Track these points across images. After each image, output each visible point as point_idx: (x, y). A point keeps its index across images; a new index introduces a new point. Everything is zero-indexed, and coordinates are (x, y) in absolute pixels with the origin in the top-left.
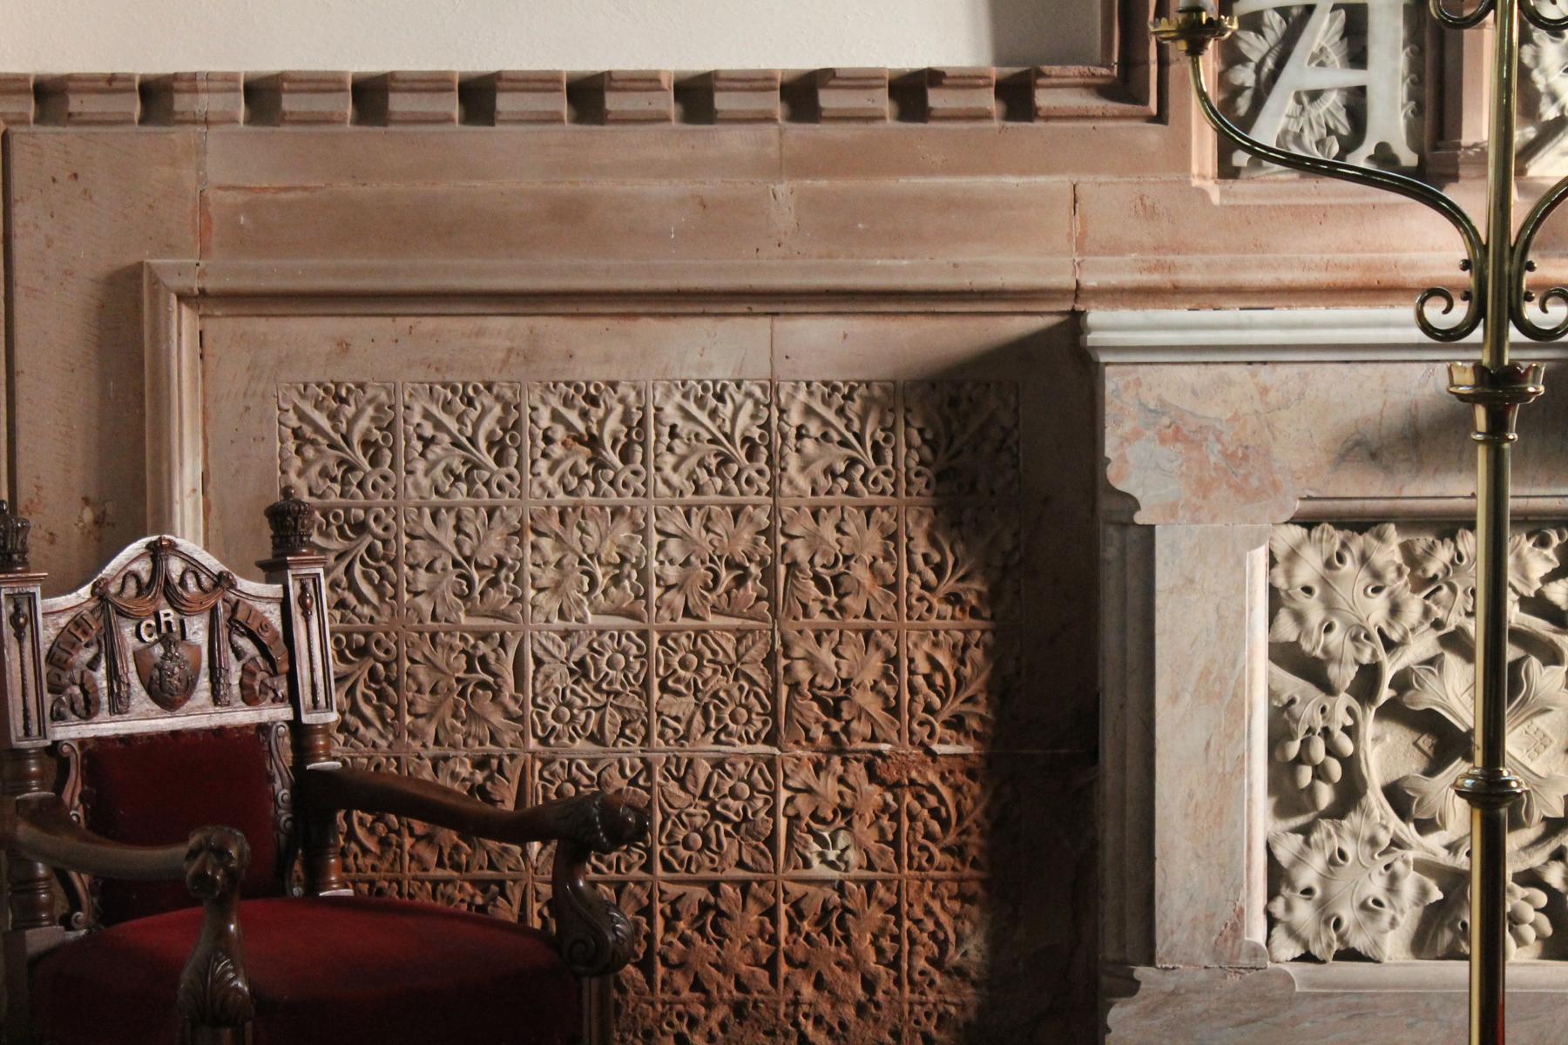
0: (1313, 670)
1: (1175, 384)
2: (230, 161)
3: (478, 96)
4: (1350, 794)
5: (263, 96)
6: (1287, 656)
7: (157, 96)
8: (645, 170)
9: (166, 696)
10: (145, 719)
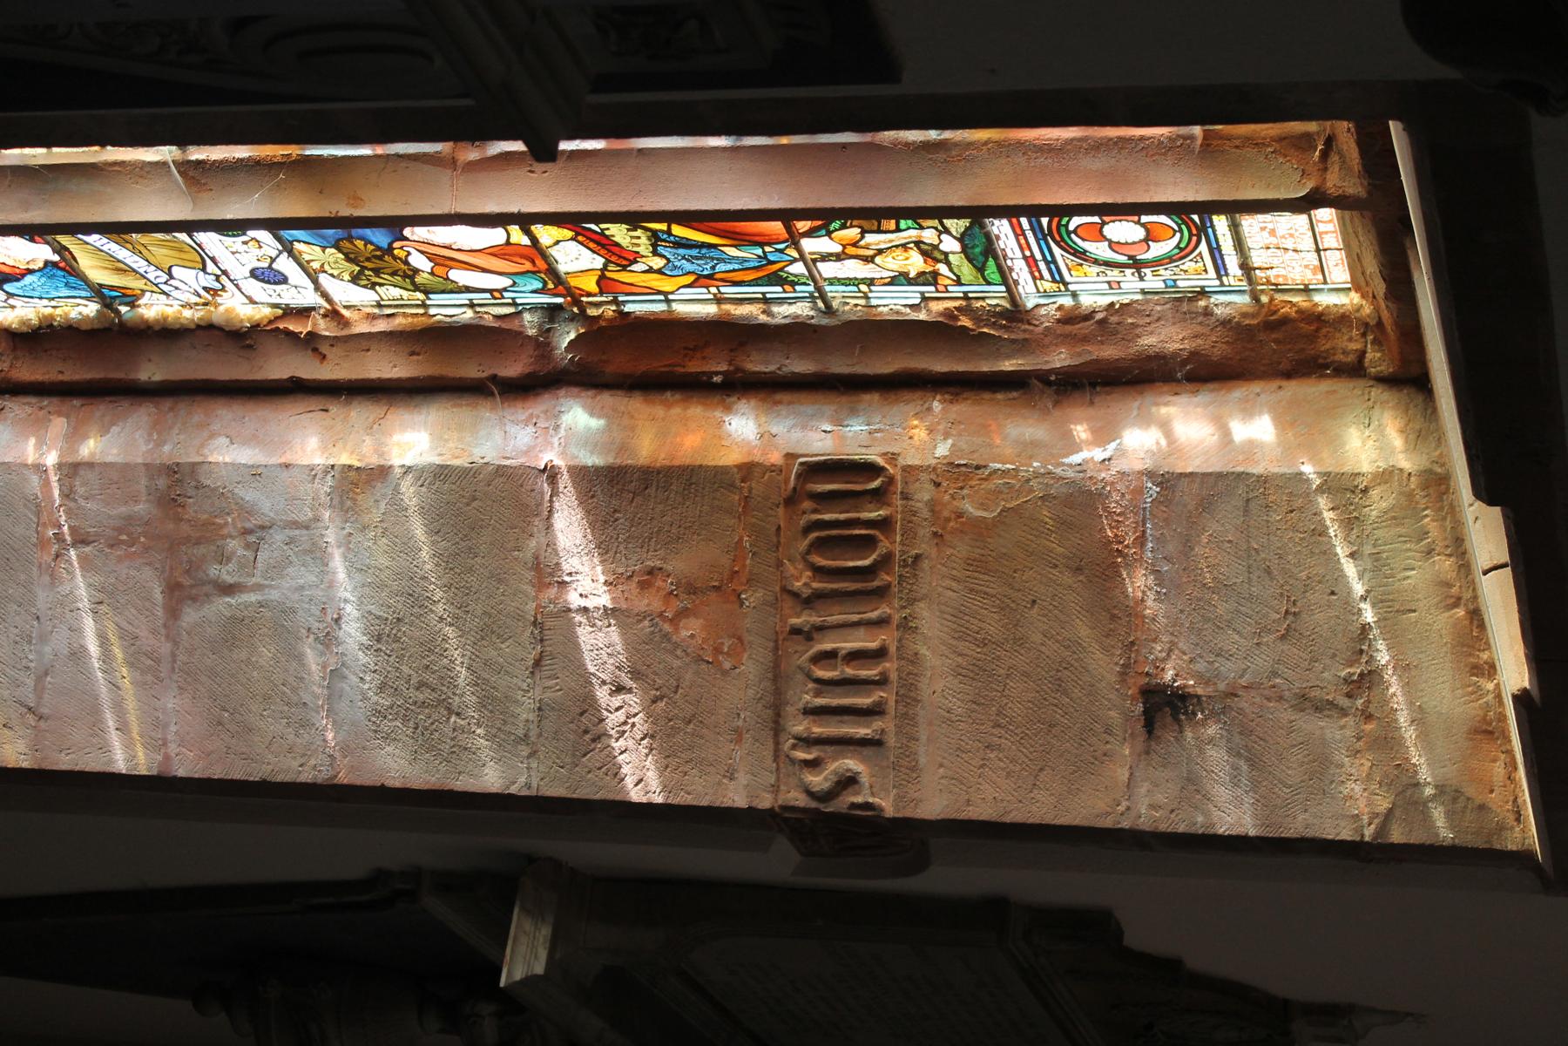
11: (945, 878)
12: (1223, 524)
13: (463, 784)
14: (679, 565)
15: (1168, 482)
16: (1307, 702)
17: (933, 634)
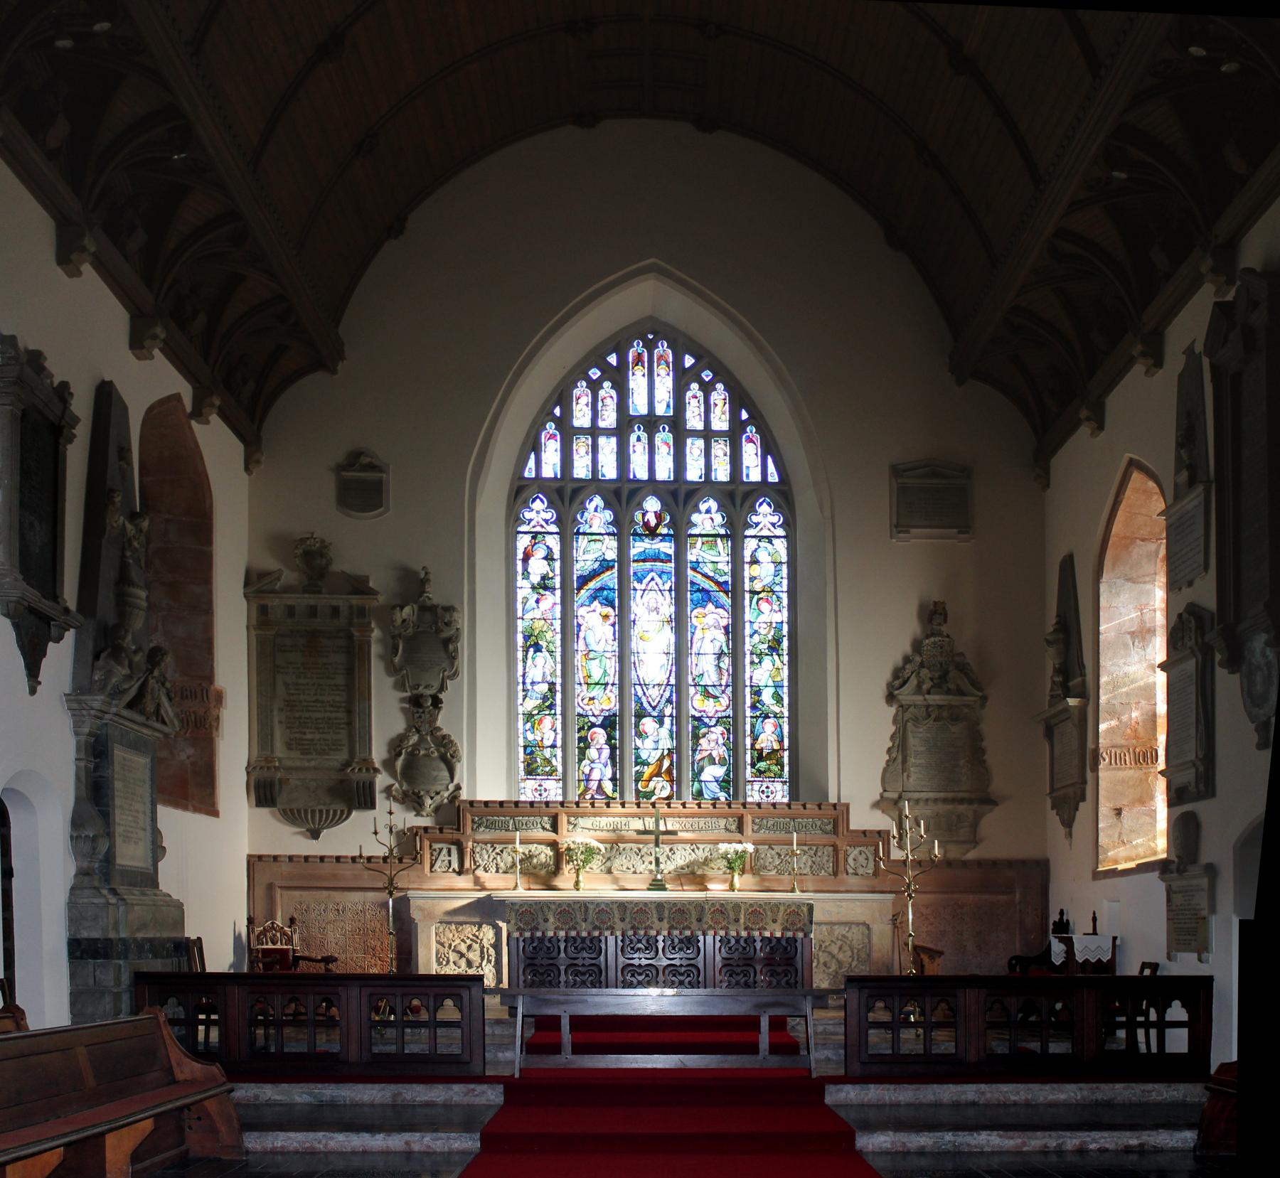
0: (442, 944)
1: (420, 902)
2: (285, 868)
3: (322, 858)
5: (291, 858)
6: (438, 942)
7: (275, 858)
8: (346, 870)
9: (274, 943)
10: (270, 946)
11: (1089, 775)
12: (1148, 819)
14: (1140, 729)
16: (1120, 834)
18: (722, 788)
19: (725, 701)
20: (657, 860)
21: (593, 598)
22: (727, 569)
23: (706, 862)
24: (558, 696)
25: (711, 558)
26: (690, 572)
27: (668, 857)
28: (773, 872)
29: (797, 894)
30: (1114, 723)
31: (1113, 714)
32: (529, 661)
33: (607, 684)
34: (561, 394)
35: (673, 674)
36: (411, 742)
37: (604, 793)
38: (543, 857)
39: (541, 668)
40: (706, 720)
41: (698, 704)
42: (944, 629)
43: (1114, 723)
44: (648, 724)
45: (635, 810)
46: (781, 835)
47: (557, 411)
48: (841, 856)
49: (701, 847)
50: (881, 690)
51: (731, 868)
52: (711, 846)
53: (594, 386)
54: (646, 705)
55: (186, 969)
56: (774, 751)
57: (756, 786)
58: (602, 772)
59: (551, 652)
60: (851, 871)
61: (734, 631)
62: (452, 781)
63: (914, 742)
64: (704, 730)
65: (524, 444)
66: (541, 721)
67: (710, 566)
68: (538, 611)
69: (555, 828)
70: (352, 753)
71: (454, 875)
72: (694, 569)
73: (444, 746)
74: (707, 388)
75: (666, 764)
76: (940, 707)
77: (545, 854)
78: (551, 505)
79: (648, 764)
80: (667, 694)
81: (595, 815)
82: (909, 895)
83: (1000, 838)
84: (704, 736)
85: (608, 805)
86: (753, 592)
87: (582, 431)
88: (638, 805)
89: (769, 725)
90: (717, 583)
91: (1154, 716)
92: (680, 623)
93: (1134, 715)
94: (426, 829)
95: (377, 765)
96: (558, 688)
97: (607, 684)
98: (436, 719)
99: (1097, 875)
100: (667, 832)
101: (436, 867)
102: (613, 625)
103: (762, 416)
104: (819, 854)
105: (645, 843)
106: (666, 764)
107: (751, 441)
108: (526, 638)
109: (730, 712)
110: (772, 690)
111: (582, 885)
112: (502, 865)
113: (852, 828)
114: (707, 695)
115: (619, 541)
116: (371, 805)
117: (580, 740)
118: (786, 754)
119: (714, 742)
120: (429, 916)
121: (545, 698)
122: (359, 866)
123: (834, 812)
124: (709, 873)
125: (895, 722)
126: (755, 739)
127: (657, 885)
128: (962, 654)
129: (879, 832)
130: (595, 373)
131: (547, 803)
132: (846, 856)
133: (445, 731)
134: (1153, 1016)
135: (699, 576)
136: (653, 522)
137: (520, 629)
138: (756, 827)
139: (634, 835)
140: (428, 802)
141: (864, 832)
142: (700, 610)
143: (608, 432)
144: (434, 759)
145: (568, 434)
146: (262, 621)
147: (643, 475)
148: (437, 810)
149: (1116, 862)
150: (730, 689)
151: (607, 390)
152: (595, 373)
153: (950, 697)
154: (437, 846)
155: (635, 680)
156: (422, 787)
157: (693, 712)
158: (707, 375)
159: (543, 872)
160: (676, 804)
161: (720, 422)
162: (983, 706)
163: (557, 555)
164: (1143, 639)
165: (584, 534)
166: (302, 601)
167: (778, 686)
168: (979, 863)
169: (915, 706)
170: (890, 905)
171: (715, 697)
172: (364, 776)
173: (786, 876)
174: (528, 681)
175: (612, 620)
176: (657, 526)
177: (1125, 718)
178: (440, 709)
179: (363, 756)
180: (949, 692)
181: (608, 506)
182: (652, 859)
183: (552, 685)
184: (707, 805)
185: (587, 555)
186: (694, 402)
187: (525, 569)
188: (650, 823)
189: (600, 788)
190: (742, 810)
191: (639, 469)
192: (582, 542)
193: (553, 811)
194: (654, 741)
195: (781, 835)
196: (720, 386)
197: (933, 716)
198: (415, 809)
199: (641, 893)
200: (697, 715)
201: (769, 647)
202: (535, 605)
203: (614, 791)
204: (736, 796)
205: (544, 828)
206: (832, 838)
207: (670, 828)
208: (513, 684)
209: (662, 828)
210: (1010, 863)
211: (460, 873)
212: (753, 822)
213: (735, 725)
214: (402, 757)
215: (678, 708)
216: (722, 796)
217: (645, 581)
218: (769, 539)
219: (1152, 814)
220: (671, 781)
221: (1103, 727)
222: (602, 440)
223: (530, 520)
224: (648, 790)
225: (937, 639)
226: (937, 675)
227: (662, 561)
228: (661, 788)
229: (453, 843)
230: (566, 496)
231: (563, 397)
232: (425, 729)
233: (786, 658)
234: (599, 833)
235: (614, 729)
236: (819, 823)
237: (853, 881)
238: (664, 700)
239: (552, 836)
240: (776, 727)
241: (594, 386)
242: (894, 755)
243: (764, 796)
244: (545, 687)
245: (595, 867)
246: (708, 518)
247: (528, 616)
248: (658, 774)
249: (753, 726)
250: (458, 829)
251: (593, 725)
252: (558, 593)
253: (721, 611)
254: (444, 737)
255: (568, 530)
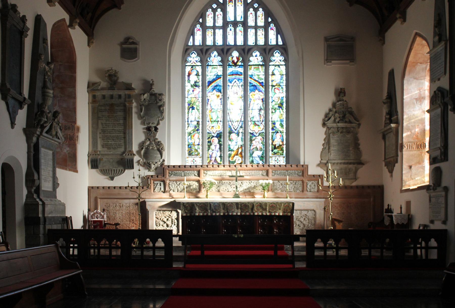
0: (158, 218)
4: (160, 225)
8: (123, 192)
12: (422, 170)
13: (404, 121)
14: (419, 135)
15: (424, 167)
16: (411, 176)
17: (415, 152)
18: (261, 160)
19: (262, 127)
20: (236, 187)
21: (214, 89)
22: (263, 77)
23: (255, 187)
24: (200, 126)
25: (257, 73)
26: (249, 79)
27: (240, 185)
28: (280, 191)
29: (288, 200)
30: (409, 133)
31: (409, 130)
32: (190, 113)
33: (218, 121)
34: (202, 14)
35: (243, 117)
36: (147, 144)
37: (217, 162)
38: (194, 186)
39: (195, 115)
40: (255, 134)
41: (252, 128)
42: (344, 98)
43: (409, 133)
44: (233, 136)
45: (228, 168)
46: (283, 177)
47: (201, 20)
48: (305, 184)
49: (253, 181)
50: (321, 122)
51: (264, 189)
52: (256, 181)
53: (214, 11)
54: (233, 129)
55: (66, 228)
56: (280, 145)
57: (273, 158)
58: (216, 154)
59: (198, 110)
60: (308, 190)
61: (266, 101)
62: (162, 158)
63: (333, 141)
64: (254, 138)
65: (188, 33)
66: (194, 135)
67: (257, 76)
68: (193, 95)
69: (199, 175)
70: (125, 148)
71: (162, 193)
72: (251, 78)
73: (159, 145)
74: (256, 10)
75: (240, 150)
76: (343, 128)
77: (195, 185)
78: (198, 55)
79: (233, 151)
80: (240, 125)
81: (214, 170)
82: (331, 199)
83: (365, 177)
84: (254, 140)
85: (218, 166)
86: (273, 86)
87: (210, 27)
88: (230, 166)
89: (278, 135)
90: (259, 83)
91: (424, 131)
92: (245, 98)
93: (417, 130)
94: (152, 176)
95: (135, 153)
96: (200, 123)
97: (218, 121)
98: (155, 136)
99: (402, 191)
100: (240, 176)
101: (156, 190)
102: (221, 99)
103: (276, 20)
104: (297, 184)
105: (232, 180)
106: (240, 150)
107: (272, 29)
108: (189, 105)
109: (264, 131)
110: (280, 122)
111: (209, 196)
112: (179, 189)
113: (309, 173)
114: (255, 124)
115: (223, 68)
116: (132, 167)
117: (208, 142)
118: (285, 146)
119: (258, 142)
120: (153, 208)
121: (195, 127)
122: (128, 190)
123: (302, 168)
124: (256, 191)
125: (326, 133)
126: (273, 141)
127: (237, 196)
128: (351, 108)
129: (319, 176)
130: (215, 6)
131: (196, 166)
132: (307, 184)
133: (159, 140)
134: (423, 244)
135: (253, 80)
136: (236, 61)
137: (187, 101)
138: (273, 174)
139: (228, 178)
140: (153, 166)
141: (314, 176)
142: (253, 93)
143: (219, 28)
144: (155, 150)
145: (204, 28)
146: (94, 100)
147: (232, 43)
148: (156, 169)
149: (410, 186)
150: (264, 122)
151: (219, 12)
152: (215, 6)
153: (346, 124)
154: (156, 182)
155: (228, 119)
156: (150, 161)
157: (250, 131)
158: (256, 5)
159: (195, 192)
160: (243, 165)
161: (261, 22)
162: (359, 127)
163: (200, 74)
164: (420, 101)
165: (210, 65)
166: (107, 93)
167: (282, 121)
168: (357, 187)
169: (333, 128)
170: (323, 203)
171: (258, 125)
172: (130, 157)
173: (284, 192)
174: (189, 121)
175: (220, 97)
176: (237, 62)
177: (413, 131)
178: (157, 131)
179: (129, 149)
180: (346, 122)
181: (219, 55)
182: (235, 186)
183: (198, 122)
184: (255, 166)
185: (211, 74)
186: (251, 15)
187: (189, 79)
188: (234, 173)
189: (215, 160)
190: (268, 168)
191: (231, 41)
192: (210, 68)
193: (198, 169)
194: (235, 142)
195: (283, 177)
196: (261, 9)
197: (340, 131)
198: (148, 169)
199: (230, 199)
200: (252, 132)
201: (279, 106)
202: (192, 92)
203: (221, 161)
204: (266, 162)
205: (195, 175)
206: (302, 178)
207: (241, 175)
208: (184, 122)
209: (238, 175)
210: (369, 187)
211: (164, 192)
212: (272, 172)
213: (266, 136)
214: (144, 150)
215: (245, 130)
216: (261, 162)
217: (233, 83)
218: (279, 66)
219: (423, 168)
220: (242, 157)
221: (404, 135)
222: (217, 31)
223: (191, 61)
224: (233, 160)
225: (342, 102)
226: (341, 116)
227: (239, 75)
228: (238, 159)
229: (162, 181)
230: (204, 51)
231: (203, 15)
232: (152, 139)
233: (285, 110)
234: (215, 177)
235: (221, 138)
236: (297, 172)
237: (309, 194)
238: (239, 126)
239: (197, 178)
240: (281, 136)
241: (214, 11)
242: (325, 146)
243: (276, 162)
244: (196, 123)
245: (213, 189)
246: (256, 58)
247: (189, 97)
248: (237, 155)
249: (272, 136)
250: (164, 176)
251: (213, 137)
252: (201, 88)
253: (260, 93)
254: (159, 142)
255: (204, 64)
